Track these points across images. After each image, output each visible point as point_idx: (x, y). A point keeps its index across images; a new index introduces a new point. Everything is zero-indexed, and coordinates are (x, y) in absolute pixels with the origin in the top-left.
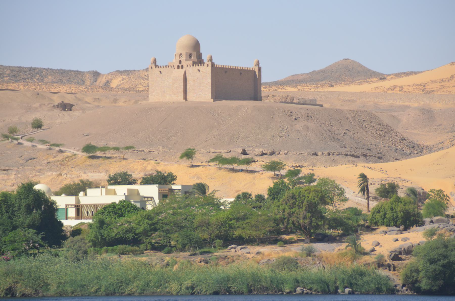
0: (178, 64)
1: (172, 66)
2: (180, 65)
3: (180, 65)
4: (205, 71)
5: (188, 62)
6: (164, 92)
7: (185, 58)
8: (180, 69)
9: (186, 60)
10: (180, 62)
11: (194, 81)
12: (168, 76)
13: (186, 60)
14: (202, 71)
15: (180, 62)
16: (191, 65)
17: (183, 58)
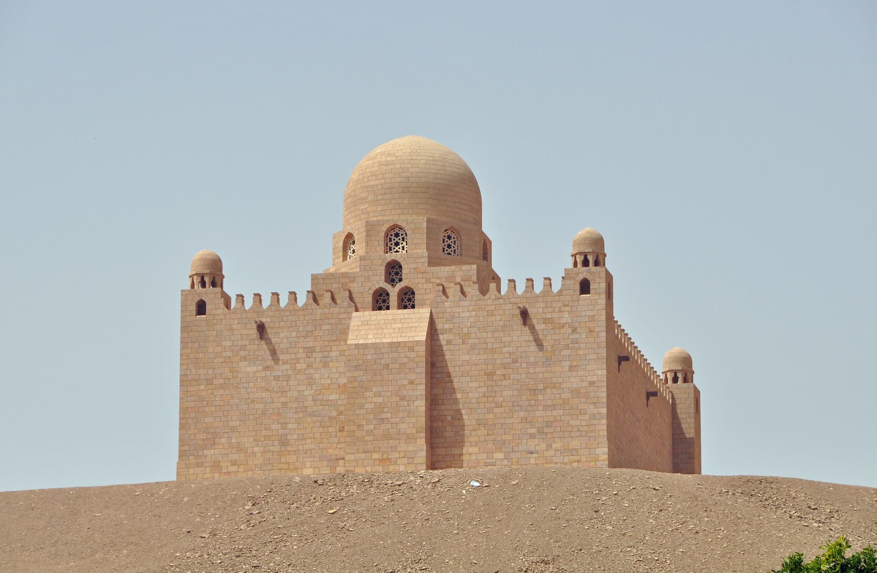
0: (380, 282)
1: (342, 297)
2: (394, 292)
3: (394, 292)
4: (566, 318)
5: (444, 271)
6: (284, 442)
7: (423, 251)
8: (394, 313)
9: (433, 262)
10: (394, 271)
11: (490, 375)
12: (310, 351)
13: (433, 262)
14: (546, 321)
15: (394, 271)
16: (473, 290)
17: (413, 254)
